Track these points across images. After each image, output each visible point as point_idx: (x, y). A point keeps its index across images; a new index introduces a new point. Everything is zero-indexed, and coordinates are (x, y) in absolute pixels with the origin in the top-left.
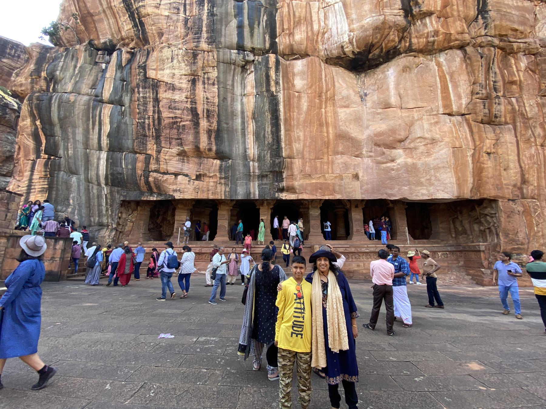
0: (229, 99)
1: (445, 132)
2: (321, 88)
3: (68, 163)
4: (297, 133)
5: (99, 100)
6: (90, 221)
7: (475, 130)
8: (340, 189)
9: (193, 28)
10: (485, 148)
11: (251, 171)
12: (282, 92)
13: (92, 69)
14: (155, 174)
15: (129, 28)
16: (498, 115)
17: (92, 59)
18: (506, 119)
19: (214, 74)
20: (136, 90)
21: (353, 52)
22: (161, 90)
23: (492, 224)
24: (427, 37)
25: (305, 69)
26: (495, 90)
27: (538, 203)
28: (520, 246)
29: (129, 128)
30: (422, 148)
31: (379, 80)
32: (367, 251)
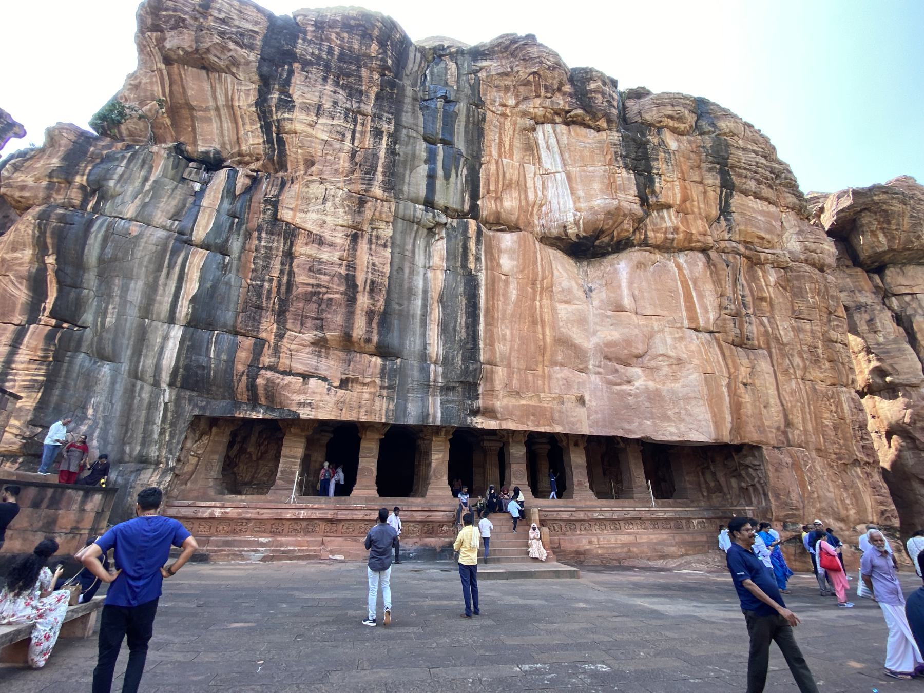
0: (407, 271)
1: (692, 351)
2: (535, 274)
3: (101, 339)
4: (502, 330)
5: (184, 240)
6: (123, 452)
7: (727, 353)
9: (364, 165)
10: (740, 378)
11: (431, 379)
12: (484, 271)
13: (176, 187)
14: (269, 374)
15: (256, 141)
17: (177, 172)
19: (387, 232)
20: (256, 234)
21: (577, 235)
23: (756, 479)
24: (665, 233)
25: (516, 246)
26: (744, 305)
28: (795, 512)
29: (233, 292)
30: (665, 370)
31: (608, 274)
32: (601, 517)
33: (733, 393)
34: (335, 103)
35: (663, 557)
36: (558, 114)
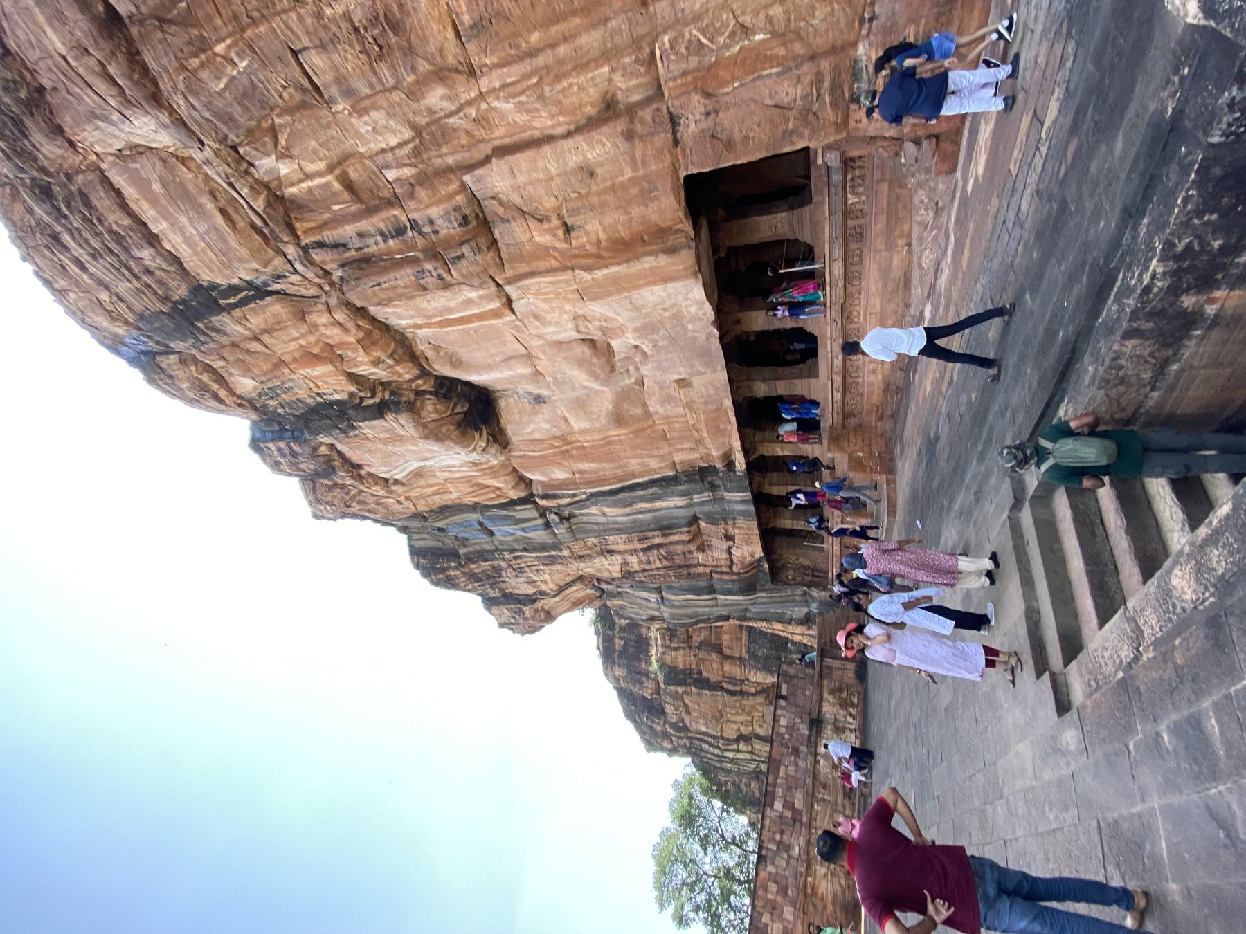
2: (555, 455)
7: (523, 268)
8: (712, 403)
9: (553, 560)
14: (735, 570)
16: (460, 219)
19: (595, 541)
24: (391, 367)
27: (666, 39)
28: (826, 85)
33: (597, 258)
35: (907, 281)
36: (359, 475)
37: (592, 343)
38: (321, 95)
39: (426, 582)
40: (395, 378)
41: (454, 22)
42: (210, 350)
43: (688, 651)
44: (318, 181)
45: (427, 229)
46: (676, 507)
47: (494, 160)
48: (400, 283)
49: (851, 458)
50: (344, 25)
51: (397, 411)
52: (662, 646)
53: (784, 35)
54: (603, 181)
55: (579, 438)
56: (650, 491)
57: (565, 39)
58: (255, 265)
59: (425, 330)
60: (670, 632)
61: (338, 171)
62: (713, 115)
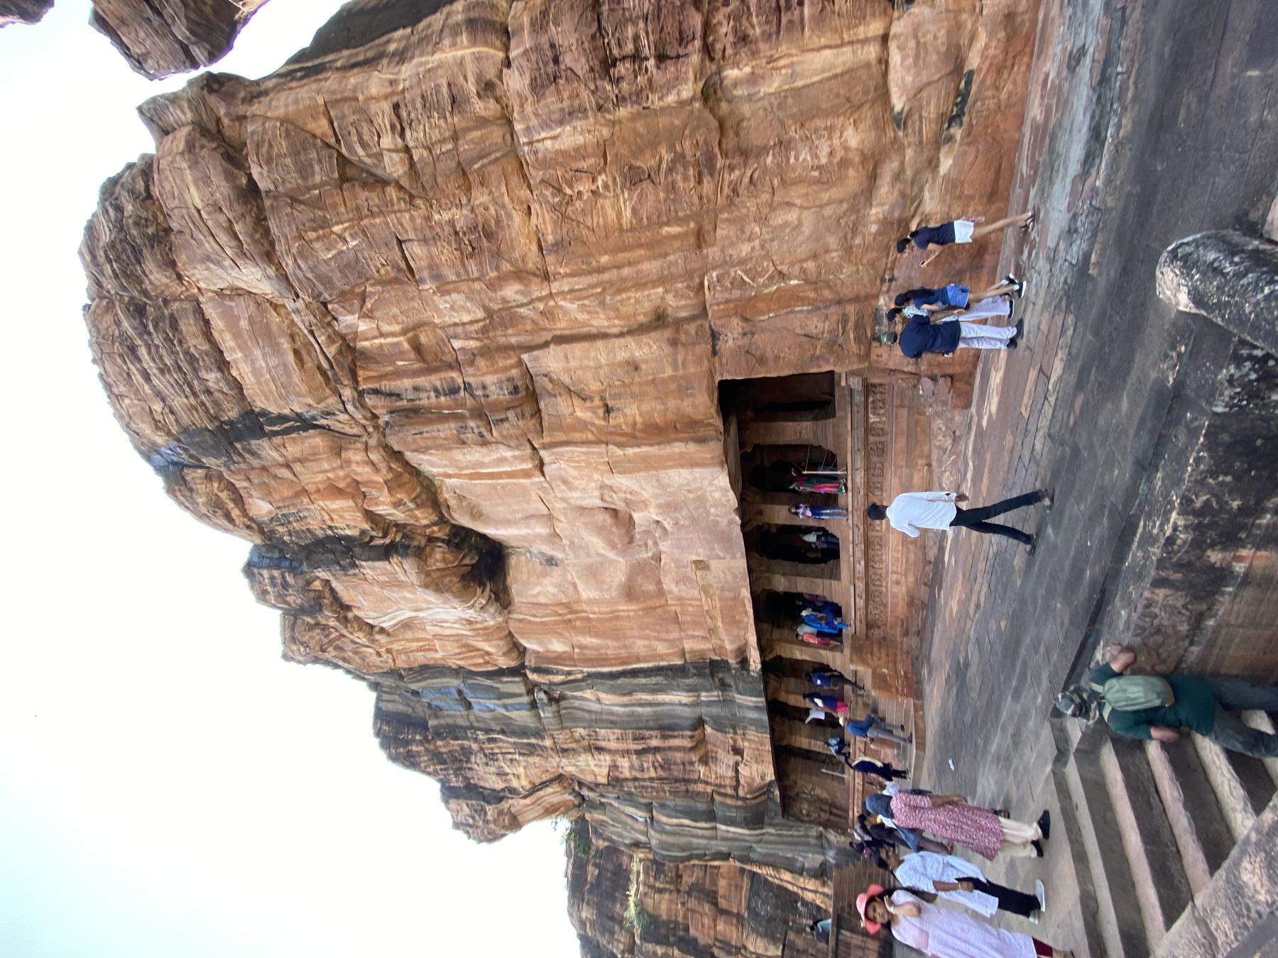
0: (611, 718)
2: (556, 623)
7: (560, 437)
9: (532, 750)
14: (741, 793)
16: (511, 388)
18: (512, 367)
19: (580, 731)
22: (621, 776)
24: (411, 510)
27: (714, 274)
28: (851, 324)
32: (863, 563)
33: (632, 437)
34: (487, 764)
36: (346, 618)
37: (615, 512)
38: (413, 276)
39: (382, 755)
40: (412, 522)
41: (539, 240)
42: (239, 470)
43: (675, 895)
44: (390, 340)
45: (479, 393)
46: (681, 704)
47: (552, 346)
48: (442, 435)
49: (874, 673)
50: (447, 228)
51: (404, 555)
52: (645, 884)
53: (815, 283)
54: (646, 375)
55: (585, 607)
56: (654, 680)
57: (630, 264)
58: (310, 401)
59: (453, 481)
60: (656, 866)
61: (410, 335)
62: (749, 336)
